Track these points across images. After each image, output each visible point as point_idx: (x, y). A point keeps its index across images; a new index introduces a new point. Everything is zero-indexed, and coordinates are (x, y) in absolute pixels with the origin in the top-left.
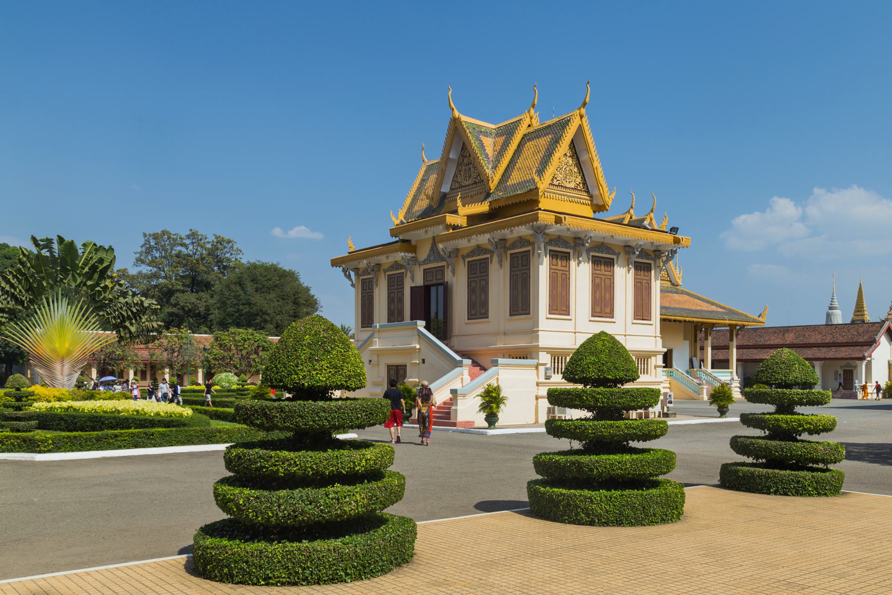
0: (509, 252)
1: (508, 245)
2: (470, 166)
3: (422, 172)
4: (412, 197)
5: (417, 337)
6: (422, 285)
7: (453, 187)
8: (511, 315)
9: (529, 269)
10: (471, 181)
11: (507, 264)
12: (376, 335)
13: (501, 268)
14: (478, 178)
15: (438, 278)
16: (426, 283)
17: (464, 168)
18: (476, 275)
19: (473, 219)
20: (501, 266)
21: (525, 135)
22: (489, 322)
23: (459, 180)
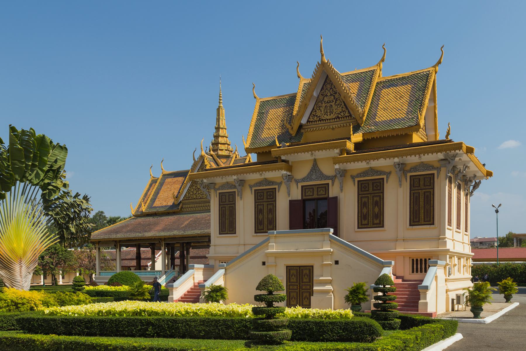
0: (409, 175)
1: (408, 168)
2: (331, 103)
3: (257, 107)
4: (253, 126)
5: (330, 242)
6: (300, 198)
7: (311, 120)
8: (410, 225)
9: (433, 189)
10: (333, 116)
11: (407, 185)
12: (272, 240)
13: (401, 187)
14: (342, 114)
15: (319, 193)
16: (304, 198)
17: (324, 105)
18: (368, 192)
19: (358, 146)
20: (400, 185)
21: (378, 83)
22: (385, 230)
23: (318, 113)
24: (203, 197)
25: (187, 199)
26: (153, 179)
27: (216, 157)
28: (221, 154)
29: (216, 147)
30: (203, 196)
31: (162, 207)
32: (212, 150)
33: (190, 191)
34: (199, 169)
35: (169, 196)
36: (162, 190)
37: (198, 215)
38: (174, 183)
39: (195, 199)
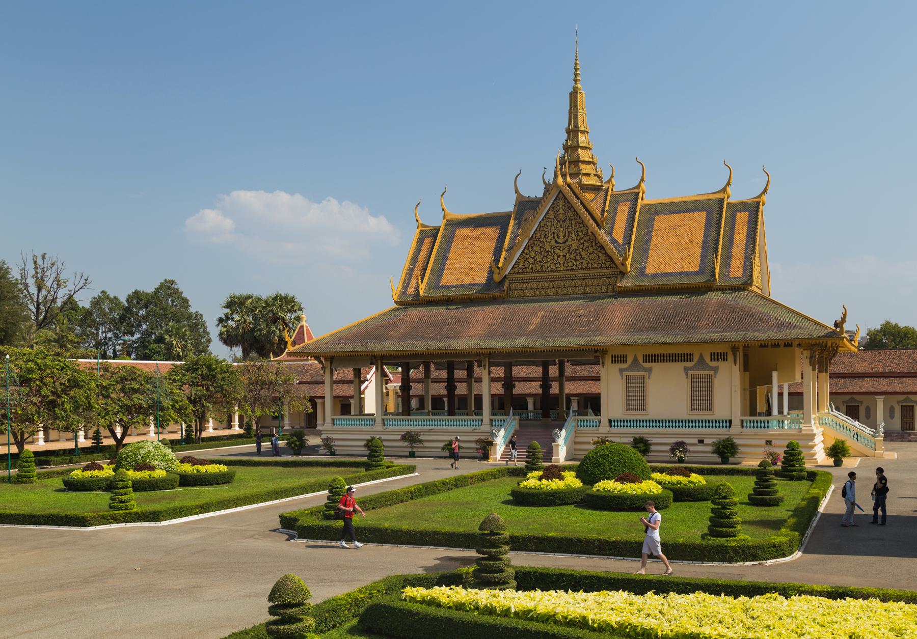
24: (559, 269)
25: (521, 271)
26: (424, 228)
27: (578, 190)
28: (587, 183)
29: (574, 169)
30: (557, 266)
31: (463, 286)
32: (569, 174)
33: (528, 256)
34: (548, 212)
35: (473, 264)
36: (452, 252)
37: (556, 306)
38: (478, 237)
39: (538, 271)
